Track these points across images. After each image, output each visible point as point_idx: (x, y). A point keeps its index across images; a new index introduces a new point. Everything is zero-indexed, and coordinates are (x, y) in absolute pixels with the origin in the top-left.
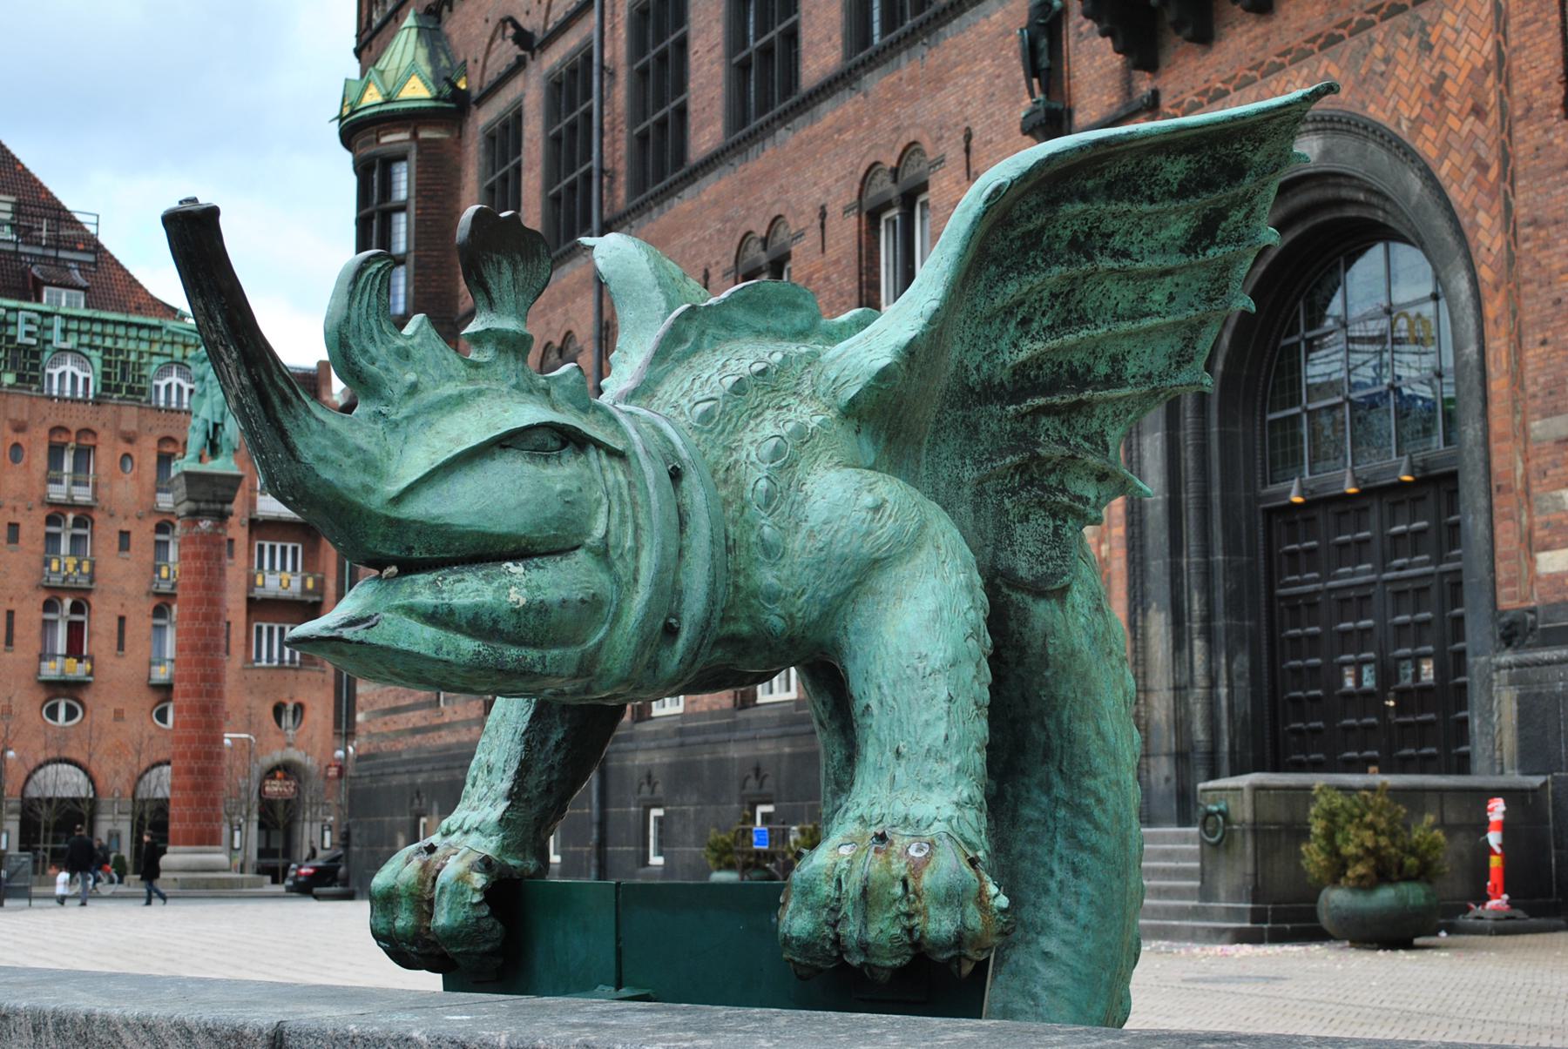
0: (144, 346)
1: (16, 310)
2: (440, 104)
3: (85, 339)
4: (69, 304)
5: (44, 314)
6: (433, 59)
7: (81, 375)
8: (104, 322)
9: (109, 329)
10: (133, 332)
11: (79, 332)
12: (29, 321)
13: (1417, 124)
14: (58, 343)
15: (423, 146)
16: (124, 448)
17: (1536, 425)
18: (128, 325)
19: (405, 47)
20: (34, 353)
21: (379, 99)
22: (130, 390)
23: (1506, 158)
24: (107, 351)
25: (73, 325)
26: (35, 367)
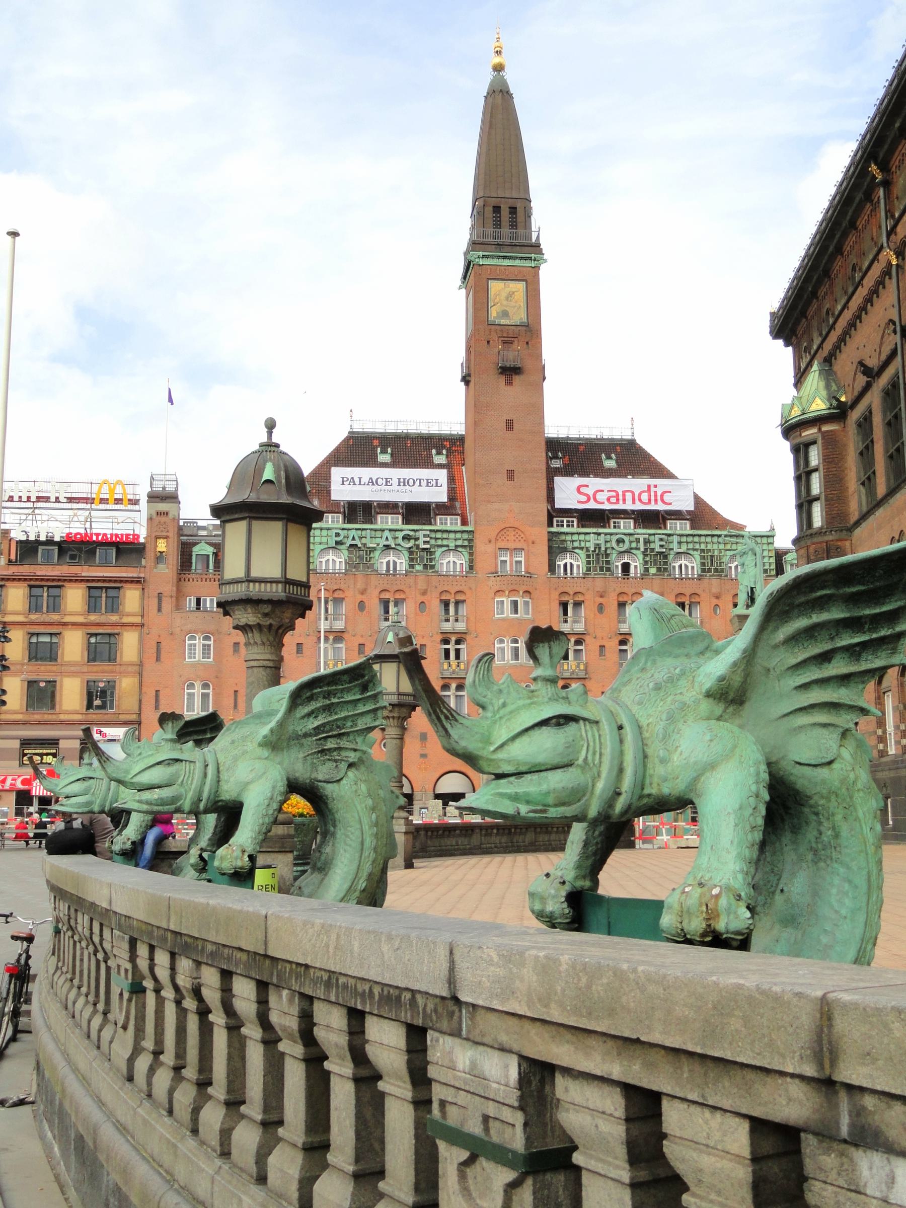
0: (722, 546)
1: (654, 535)
2: (832, 411)
3: (690, 546)
4: (681, 529)
5: (669, 535)
6: (828, 387)
7: (690, 565)
8: (700, 536)
9: (703, 539)
10: (715, 539)
11: (687, 543)
12: (661, 540)
14: (676, 550)
15: (825, 435)
16: (715, 601)
18: (713, 536)
19: (814, 379)
21: (799, 413)
22: (716, 570)
24: (703, 551)
25: (684, 539)
26: (665, 563)
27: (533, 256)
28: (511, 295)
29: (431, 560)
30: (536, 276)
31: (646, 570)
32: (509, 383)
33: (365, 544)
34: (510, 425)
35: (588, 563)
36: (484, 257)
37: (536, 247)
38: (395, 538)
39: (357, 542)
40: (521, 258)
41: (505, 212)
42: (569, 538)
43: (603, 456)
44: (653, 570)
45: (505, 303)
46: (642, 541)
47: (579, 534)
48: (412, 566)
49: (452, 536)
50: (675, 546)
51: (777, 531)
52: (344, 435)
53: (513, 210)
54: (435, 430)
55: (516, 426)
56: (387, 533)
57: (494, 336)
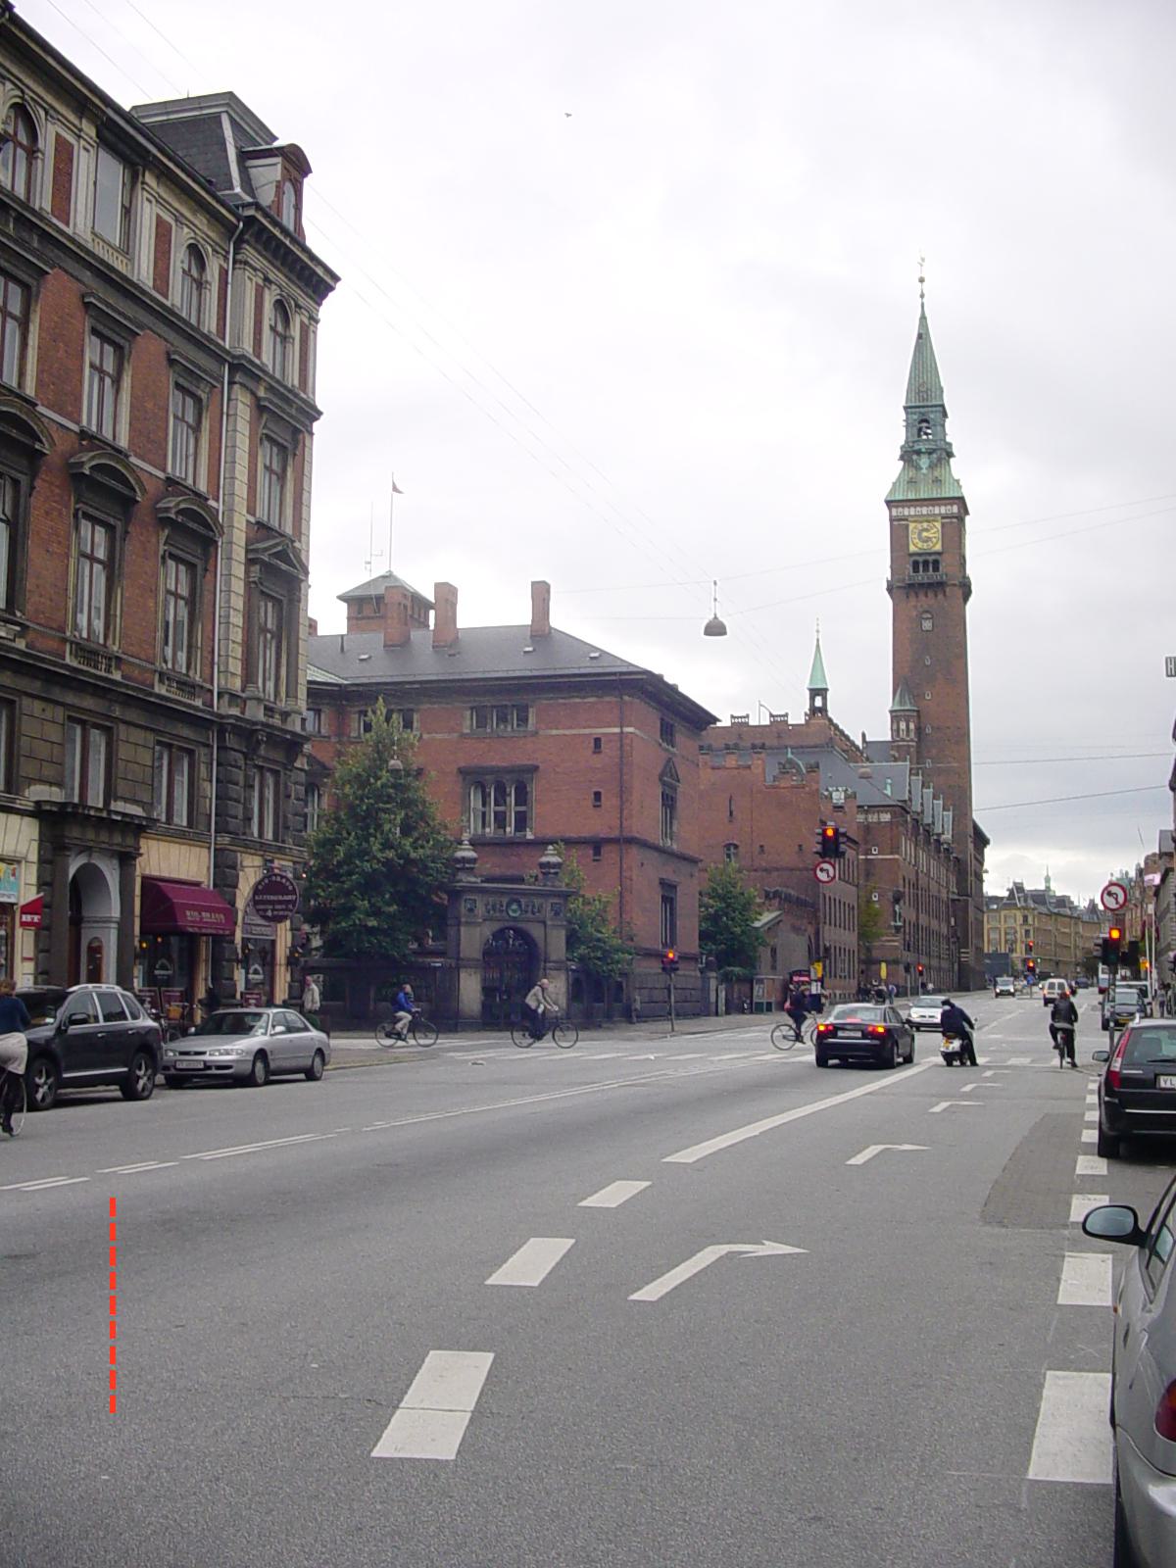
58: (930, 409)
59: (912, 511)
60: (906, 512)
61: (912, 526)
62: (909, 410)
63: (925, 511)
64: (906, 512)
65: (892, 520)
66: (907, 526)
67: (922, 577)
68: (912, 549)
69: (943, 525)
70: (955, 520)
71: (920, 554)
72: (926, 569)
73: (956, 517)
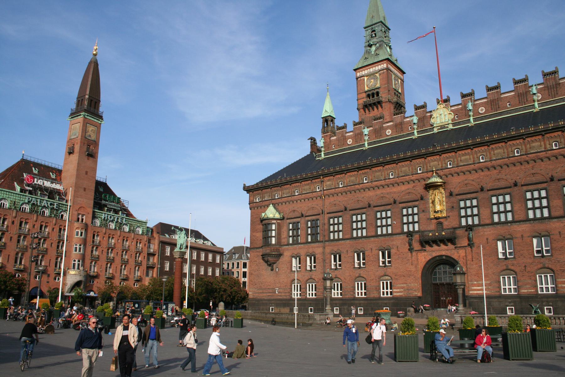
0: (135, 224)
3: (127, 222)
8: (130, 219)
13: (457, 259)
14: (124, 222)
16: (132, 240)
17: (469, 283)
19: (271, 208)
20: (121, 224)
23: (466, 263)
24: (130, 224)
26: (121, 226)
27: (101, 120)
28: (92, 130)
29: (57, 213)
30: (100, 126)
31: (116, 227)
32: (88, 159)
33: (37, 204)
34: (87, 173)
35: (101, 222)
36: (87, 116)
37: (101, 117)
38: (47, 204)
39: (35, 202)
40: (97, 119)
41: (93, 103)
42: (97, 213)
43: (99, 187)
44: (117, 228)
45: (90, 132)
46: (116, 218)
47: (100, 213)
48: (51, 214)
49: (64, 206)
50: (124, 221)
51: (148, 222)
52: (18, 159)
53: (96, 102)
54: (50, 165)
55: (88, 174)
56: (45, 202)
57: (86, 142)
58: (376, 25)
59: (366, 72)
60: (363, 73)
61: (366, 78)
62: (367, 29)
63: (371, 70)
64: (363, 73)
65: (357, 79)
66: (364, 80)
67: (372, 100)
68: (366, 89)
69: (380, 75)
70: (385, 71)
71: (370, 91)
72: (373, 97)
73: (386, 69)
